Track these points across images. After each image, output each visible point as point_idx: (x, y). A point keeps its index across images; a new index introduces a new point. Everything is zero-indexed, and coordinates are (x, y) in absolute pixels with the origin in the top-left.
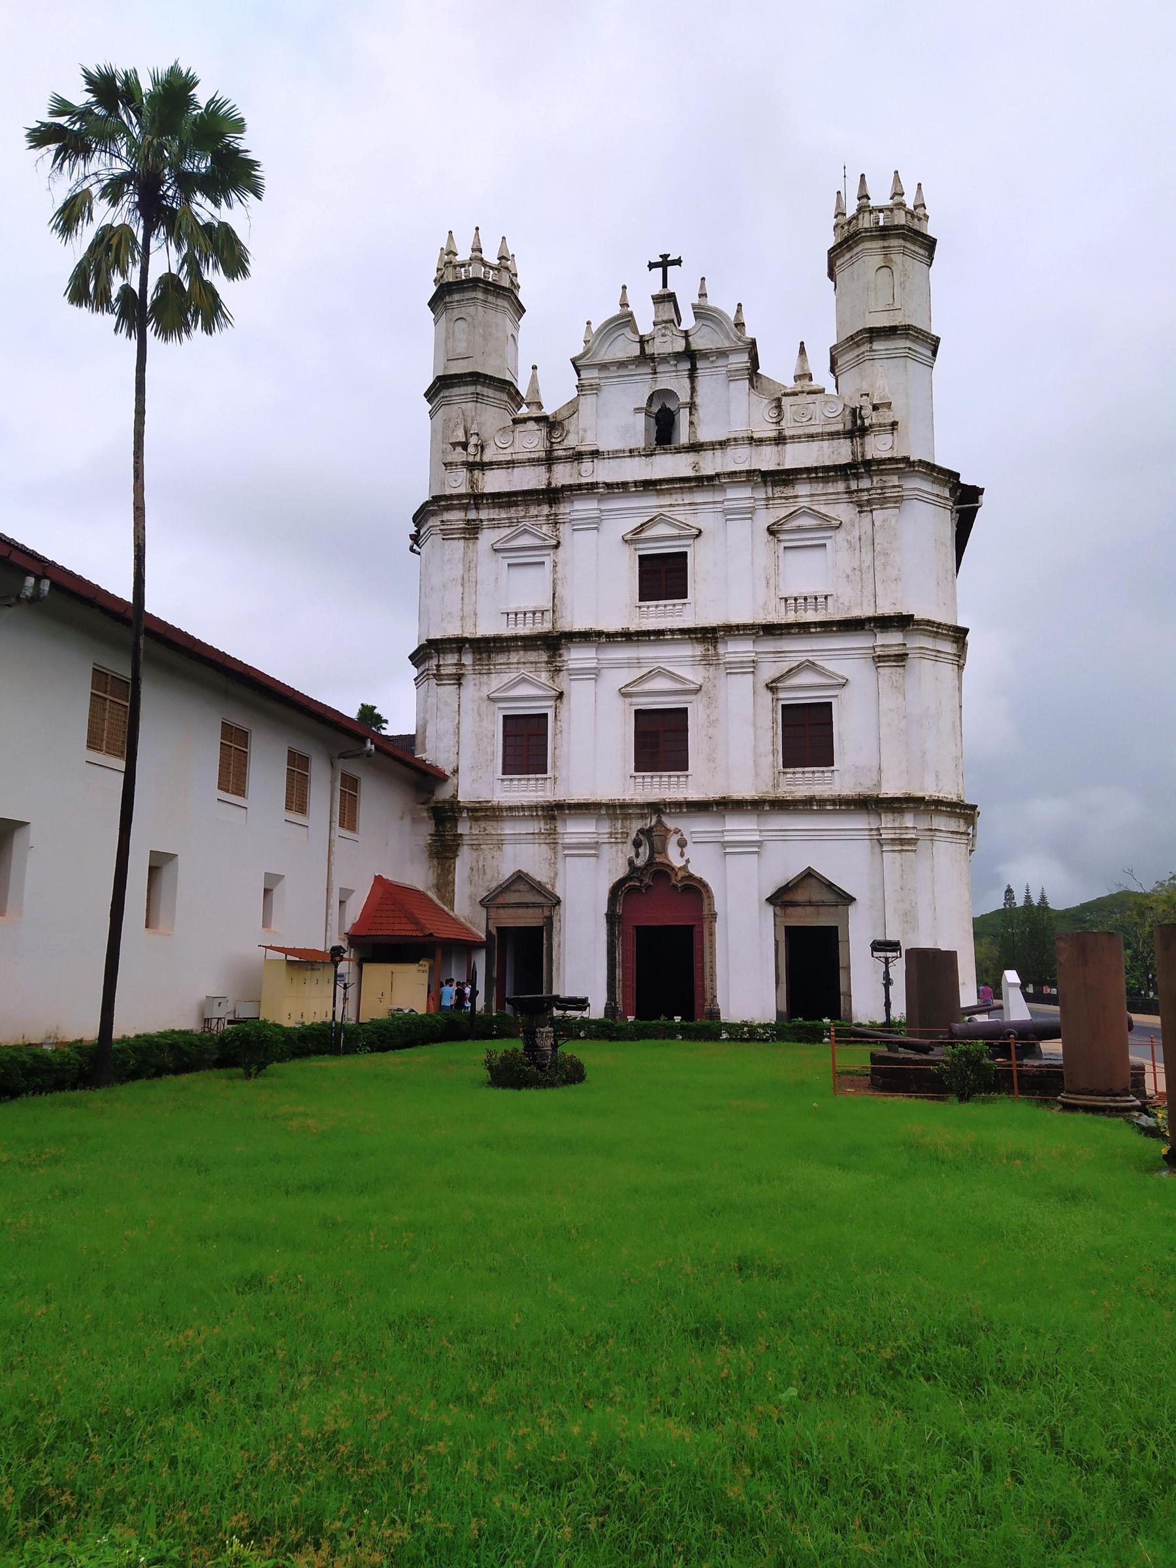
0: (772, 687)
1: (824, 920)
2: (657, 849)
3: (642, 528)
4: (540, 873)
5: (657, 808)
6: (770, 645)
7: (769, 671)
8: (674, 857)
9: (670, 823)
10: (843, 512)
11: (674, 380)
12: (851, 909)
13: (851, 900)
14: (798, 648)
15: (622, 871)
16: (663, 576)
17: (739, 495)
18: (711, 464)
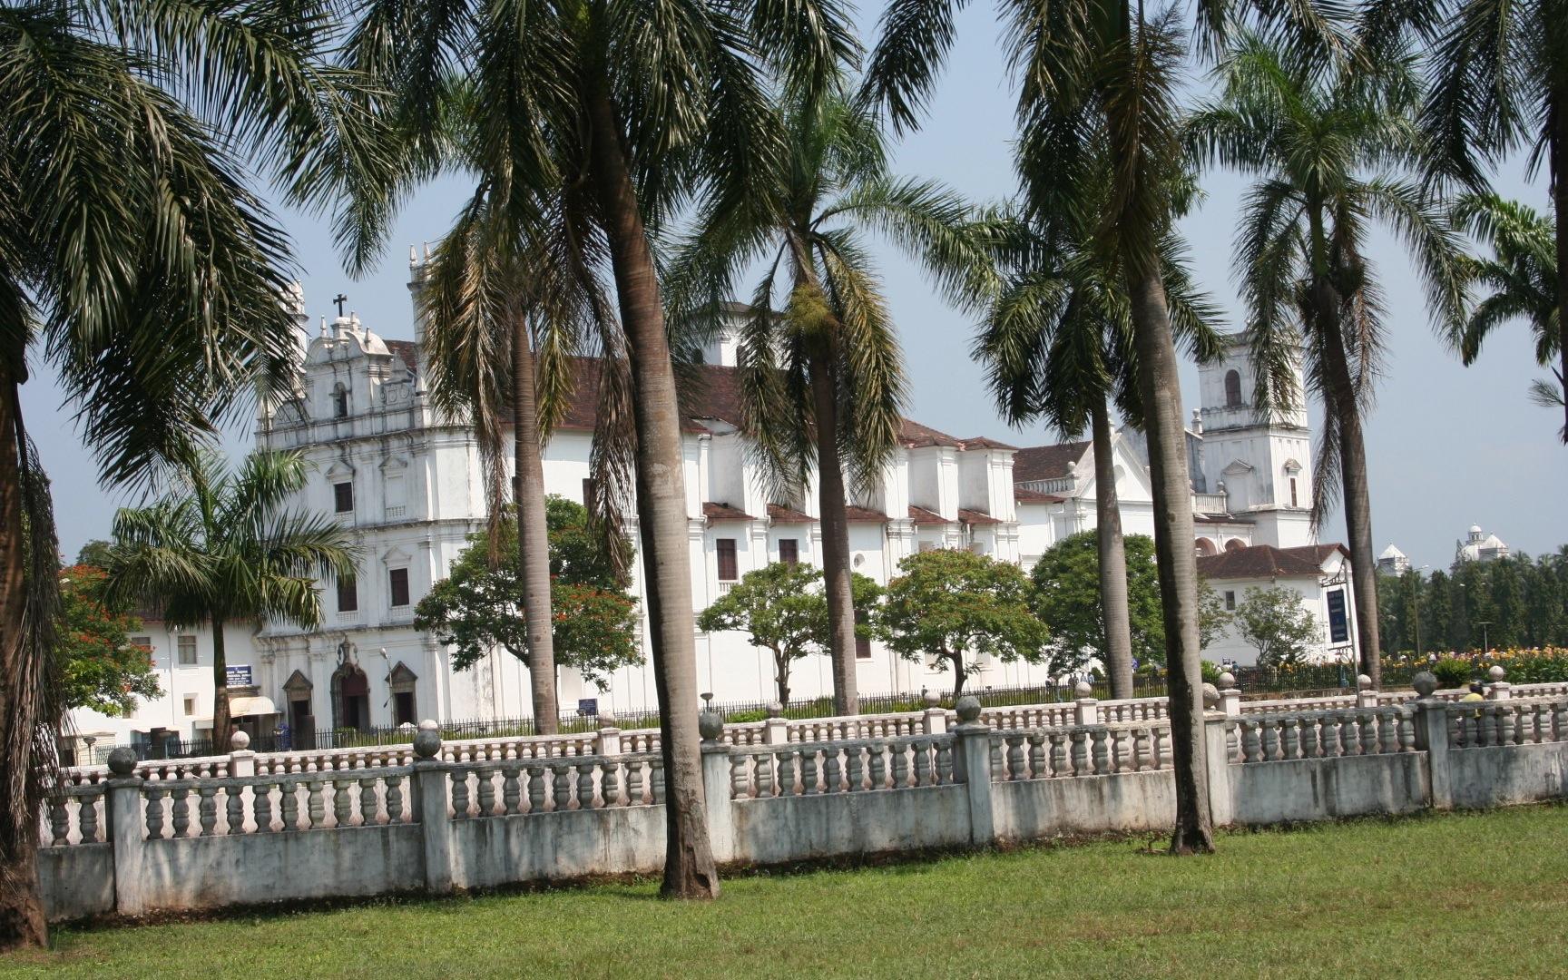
0: (384, 560)
1: (408, 690)
2: (346, 657)
3: (331, 471)
4: (304, 671)
5: (343, 632)
6: (382, 536)
7: (382, 552)
8: (353, 661)
9: (351, 640)
10: (407, 456)
11: (343, 379)
12: (418, 684)
13: (414, 678)
14: (394, 537)
15: (335, 668)
16: (344, 497)
17: (366, 448)
18: (361, 429)
